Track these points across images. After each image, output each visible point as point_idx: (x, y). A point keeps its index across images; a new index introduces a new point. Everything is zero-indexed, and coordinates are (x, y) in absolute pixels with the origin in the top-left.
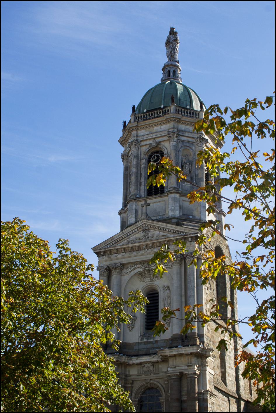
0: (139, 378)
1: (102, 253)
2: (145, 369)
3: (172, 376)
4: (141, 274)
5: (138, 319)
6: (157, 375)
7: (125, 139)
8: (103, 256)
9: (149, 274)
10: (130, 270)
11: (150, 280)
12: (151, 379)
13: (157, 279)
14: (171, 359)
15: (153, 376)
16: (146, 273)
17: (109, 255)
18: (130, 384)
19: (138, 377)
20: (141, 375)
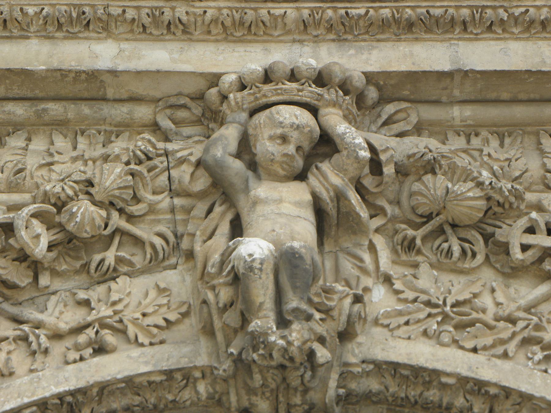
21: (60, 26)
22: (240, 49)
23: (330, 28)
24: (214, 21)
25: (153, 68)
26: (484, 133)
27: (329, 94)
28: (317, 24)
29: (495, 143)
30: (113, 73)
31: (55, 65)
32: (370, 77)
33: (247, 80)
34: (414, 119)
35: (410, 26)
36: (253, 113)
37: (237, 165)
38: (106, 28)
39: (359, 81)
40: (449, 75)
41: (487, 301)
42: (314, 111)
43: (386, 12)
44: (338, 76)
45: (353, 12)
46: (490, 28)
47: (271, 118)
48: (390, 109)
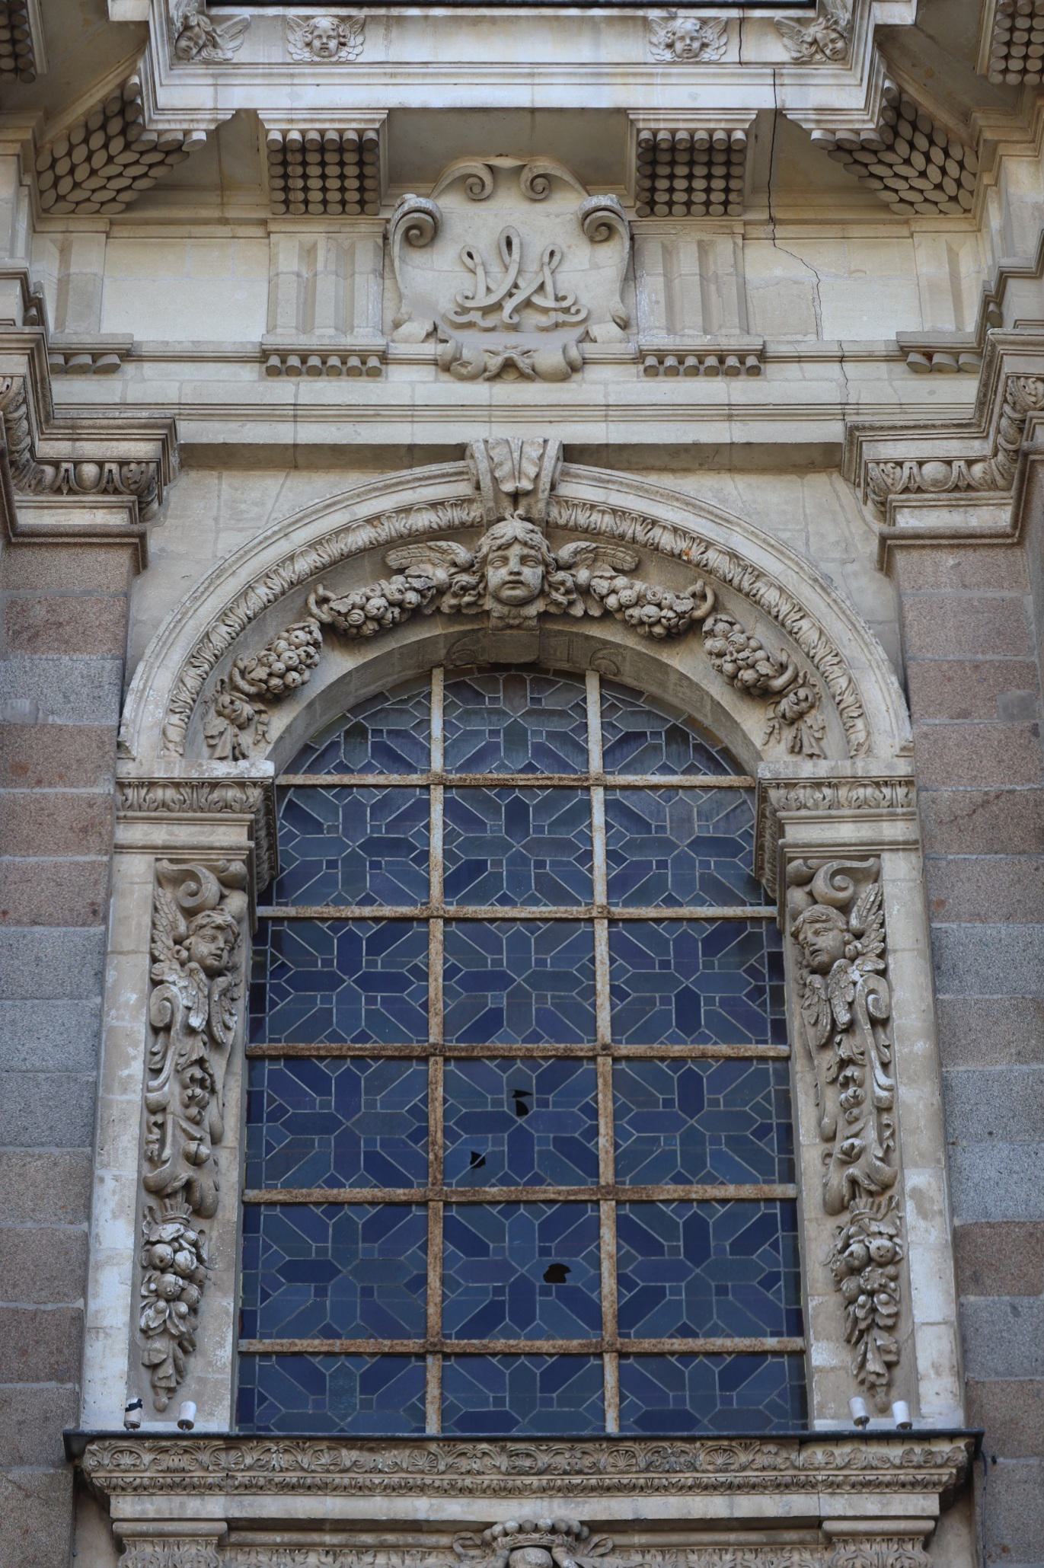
0: (297, 413)
12: (571, 453)
18: (106, 486)
19: (284, 390)
21: (394, 1489)
22: (504, 1502)
23: (559, 1490)
24: (489, 1487)
25: (451, 1518)
26: (653, 1551)
27: (558, 1539)
28: (552, 1488)
29: (659, 1558)
30: (427, 1521)
31: (392, 1516)
32: (582, 1523)
33: (509, 1530)
34: (610, 1545)
35: (608, 1489)
36: (513, 1550)
38: (422, 1490)
39: (576, 1526)
40: (633, 1521)
42: (548, 1549)
43: (593, 1482)
44: (563, 1527)
45: (574, 1482)
46: (657, 1490)
47: (523, 1558)
48: (596, 1539)
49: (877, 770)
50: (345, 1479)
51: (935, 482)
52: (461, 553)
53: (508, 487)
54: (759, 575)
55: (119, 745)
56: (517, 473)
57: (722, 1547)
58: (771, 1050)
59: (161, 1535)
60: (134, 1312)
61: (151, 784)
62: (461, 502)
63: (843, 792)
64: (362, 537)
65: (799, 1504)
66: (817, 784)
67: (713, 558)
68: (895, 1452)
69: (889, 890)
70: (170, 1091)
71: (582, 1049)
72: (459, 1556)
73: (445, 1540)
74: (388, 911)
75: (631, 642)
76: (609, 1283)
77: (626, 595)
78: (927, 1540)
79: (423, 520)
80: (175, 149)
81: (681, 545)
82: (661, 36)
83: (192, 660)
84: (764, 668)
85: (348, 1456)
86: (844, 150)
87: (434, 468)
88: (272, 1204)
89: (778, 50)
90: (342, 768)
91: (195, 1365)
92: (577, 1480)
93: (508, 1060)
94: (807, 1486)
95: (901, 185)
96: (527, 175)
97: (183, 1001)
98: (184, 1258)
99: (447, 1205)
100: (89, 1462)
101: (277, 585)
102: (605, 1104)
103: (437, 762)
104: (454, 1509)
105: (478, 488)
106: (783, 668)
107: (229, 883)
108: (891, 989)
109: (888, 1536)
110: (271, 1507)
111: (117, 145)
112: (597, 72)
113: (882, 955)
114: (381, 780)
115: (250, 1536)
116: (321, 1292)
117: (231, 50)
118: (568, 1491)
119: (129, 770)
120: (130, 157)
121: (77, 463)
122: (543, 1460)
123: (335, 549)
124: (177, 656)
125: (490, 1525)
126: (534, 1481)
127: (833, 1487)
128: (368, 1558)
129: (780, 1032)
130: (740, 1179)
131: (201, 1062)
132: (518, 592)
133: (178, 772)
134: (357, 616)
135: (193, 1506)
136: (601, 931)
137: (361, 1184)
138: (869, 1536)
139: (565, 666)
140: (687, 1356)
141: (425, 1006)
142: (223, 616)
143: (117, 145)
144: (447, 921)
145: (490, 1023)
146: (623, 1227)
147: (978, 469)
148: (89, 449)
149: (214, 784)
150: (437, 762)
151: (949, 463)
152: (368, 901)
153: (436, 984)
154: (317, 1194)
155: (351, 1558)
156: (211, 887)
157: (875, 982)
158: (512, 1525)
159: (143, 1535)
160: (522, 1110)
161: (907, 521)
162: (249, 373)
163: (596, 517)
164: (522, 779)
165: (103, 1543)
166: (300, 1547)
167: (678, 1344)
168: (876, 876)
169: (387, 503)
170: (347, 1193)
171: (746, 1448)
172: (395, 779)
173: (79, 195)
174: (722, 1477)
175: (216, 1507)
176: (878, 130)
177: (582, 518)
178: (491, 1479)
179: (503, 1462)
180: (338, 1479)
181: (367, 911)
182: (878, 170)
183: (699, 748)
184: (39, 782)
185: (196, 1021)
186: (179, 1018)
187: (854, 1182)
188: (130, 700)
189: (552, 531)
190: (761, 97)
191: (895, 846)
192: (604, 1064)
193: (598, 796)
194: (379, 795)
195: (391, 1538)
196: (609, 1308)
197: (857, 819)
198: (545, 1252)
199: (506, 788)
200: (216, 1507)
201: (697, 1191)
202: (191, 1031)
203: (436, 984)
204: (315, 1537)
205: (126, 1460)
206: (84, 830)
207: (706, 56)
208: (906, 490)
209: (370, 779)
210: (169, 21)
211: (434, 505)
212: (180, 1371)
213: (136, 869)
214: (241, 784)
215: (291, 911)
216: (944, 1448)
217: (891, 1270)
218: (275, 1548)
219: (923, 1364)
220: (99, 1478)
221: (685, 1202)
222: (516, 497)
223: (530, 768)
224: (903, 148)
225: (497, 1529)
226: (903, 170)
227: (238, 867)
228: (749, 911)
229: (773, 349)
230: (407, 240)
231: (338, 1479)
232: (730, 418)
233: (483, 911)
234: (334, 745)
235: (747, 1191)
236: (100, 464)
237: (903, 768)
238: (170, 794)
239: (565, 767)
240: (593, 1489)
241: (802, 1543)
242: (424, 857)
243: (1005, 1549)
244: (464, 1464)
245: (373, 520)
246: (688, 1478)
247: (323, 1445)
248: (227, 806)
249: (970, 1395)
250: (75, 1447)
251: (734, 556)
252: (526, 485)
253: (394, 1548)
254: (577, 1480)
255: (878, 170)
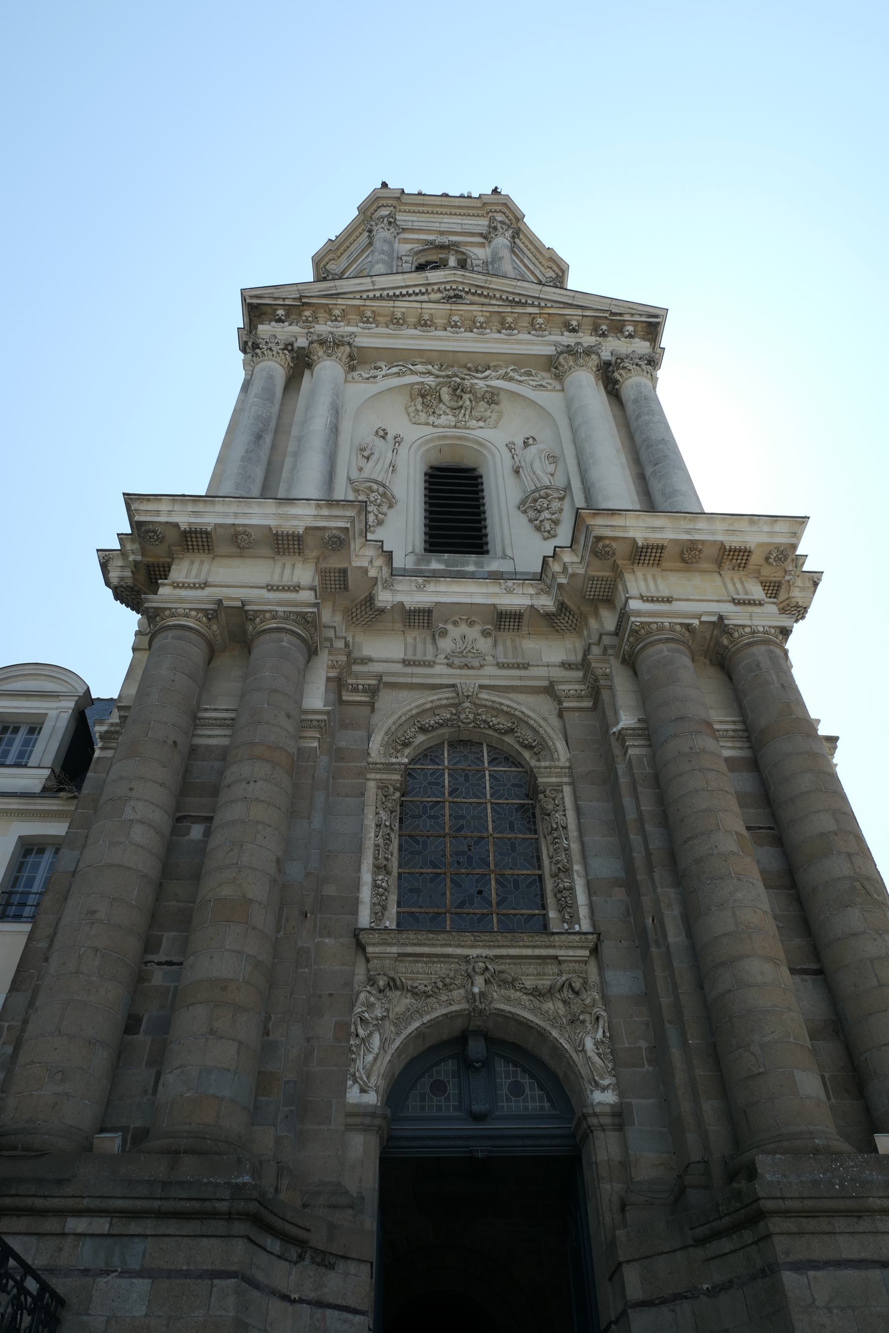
0: (412, 675)
1: (281, 312)
2: (446, 644)
3: (661, 629)
4: (423, 396)
5: (399, 507)
6: (516, 672)
7: (338, 249)
8: (280, 320)
9: (454, 404)
10: (384, 373)
11: (453, 424)
12: (481, 687)
13: (481, 424)
14: (639, 574)
15: (490, 674)
16: (446, 397)
17: (307, 321)
18: (365, 691)
19: (409, 670)
20: (430, 664)
37: (472, 973)
41: (512, 996)
49: (561, 764)
50: (430, 942)
51: (573, 695)
52: (454, 711)
53: (466, 694)
54: (529, 717)
55: (368, 754)
56: (468, 690)
57: (531, 964)
58: (533, 836)
59: (379, 957)
60: (372, 898)
61: (376, 764)
62: (453, 698)
63: (552, 770)
64: (429, 706)
65: (552, 952)
66: (546, 768)
67: (517, 713)
68: (577, 938)
69: (565, 794)
70: (380, 841)
71: (485, 835)
72: (460, 965)
73: (456, 960)
74: (434, 799)
75: (495, 734)
76: (494, 895)
77: (495, 722)
78: (586, 962)
79: (444, 702)
80: (382, 611)
81: (509, 710)
82: (503, 586)
83: (386, 734)
84: (530, 740)
85: (431, 936)
86: (548, 617)
87: (447, 690)
88: (405, 873)
89: (531, 591)
90: (422, 764)
91: (386, 914)
92: (492, 944)
93: (466, 838)
94: (554, 947)
95: (562, 625)
96: (469, 621)
97: (384, 818)
98: (384, 884)
99: (451, 874)
100: (361, 937)
101: (407, 716)
102: (491, 849)
103: (446, 763)
104: (459, 951)
105: (458, 694)
106: (535, 740)
107: (396, 789)
108: (567, 819)
109: (576, 962)
110: (410, 950)
111: (368, 609)
112: (487, 595)
113: (564, 811)
114: (432, 767)
115: (404, 958)
116: (418, 896)
117: (398, 587)
118: (489, 947)
119: (370, 760)
120: (371, 613)
121: (358, 685)
122: (483, 938)
123: (422, 708)
124: (383, 733)
125: (469, 956)
126: (480, 943)
127: (560, 947)
128: (435, 965)
129: (535, 832)
130: (529, 869)
131: (389, 834)
132: (468, 721)
133: (383, 761)
134: (427, 725)
135: (389, 949)
136: (489, 806)
137: (429, 868)
138: (571, 961)
139: (478, 741)
140: (515, 915)
141: (444, 823)
142: (394, 723)
143: (368, 609)
144: (450, 802)
145: (461, 828)
146: (497, 881)
147: (583, 692)
148: (360, 681)
149: (393, 764)
150: (446, 763)
151: (576, 691)
152: (429, 797)
153: (447, 818)
154: (417, 870)
155: (431, 965)
156: (391, 790)
157: (562, 817)
158: (475, 956)
159: (375, 957)
160: (470, 850)
161: (565, 704)
162: (400, 666)
163: (487, 703)
164: (468, 768)
165: (363, 960)
166: (417, 962)
167: (512, 912)
168: (562, 791)
169: (435, 698)
170: (424, 871)
171: (537, 936)
172: (436, 767)
173: (358, 622)
174: (531, 944)
175: (395, 950)
176: (557, 611)
177: (484, 703)
178: (469, 943)
179: (472, 938)
180: (428, 942)
181: (429, 799)
182: (557, 621)
183: (512, 762)
184: (348, 762)
185: (387, 823)
186: (383, 822)
187: (559, 869)
188: (371, 742)
189: (475, 704)
190: (527, 602)
191: (566, 783)
192: (491, 839)
193: (487, 773)
194: (432, 771)
195: (442, 959)
196: (494, 902)
197: (556, 777)
198: (477, 887)
199: (463, 770)
200: (395, 950)
201: (516, 872)
202: (386, 826)
203: (447, 818)
204: (421, 959)
205: (371, 936)
206: (359, 774)
207: (515, 592)
208: (565, 697)
209: (429, 767)
210: (382, 579)
211: (447, 699)
212: (383, 915)
213: (372, 785)
214: (399, 764)
215: (410, 799)
216: (590, 937)
217: (571, 891)
218: (410, 962)
219: (581, 916)
220: (363, 941)
221: (513, 875)
222: (468, 696)
223: (469, 765)
224: (563, 615)
225: (471, 957)
226: (562, 621)
227: (398, 785)
228: (527, 802)
229: (531, 663)
230: (439, 635)
231: (428, 942)
232: (520, 679)
233: (459, 800)
234: (420, 759)
235: (529, 872)
236: (363, 686)
237: (568, 764)
238: (381, 766)
239: (479, 765)
240: (496, 946)
241: (552, 963)
242: (444, 786)
243: (608, 966)
244: (461, 938)
245: (432, 702)
246: (521, 944)
247: (424, 933)
248: (396, 770)
249: (594, 923)
250: (357, 932)
251: (522, 712)
252: (471, 694)
253: (443, 962)
254: (492, 944)
255: (557, 621)
